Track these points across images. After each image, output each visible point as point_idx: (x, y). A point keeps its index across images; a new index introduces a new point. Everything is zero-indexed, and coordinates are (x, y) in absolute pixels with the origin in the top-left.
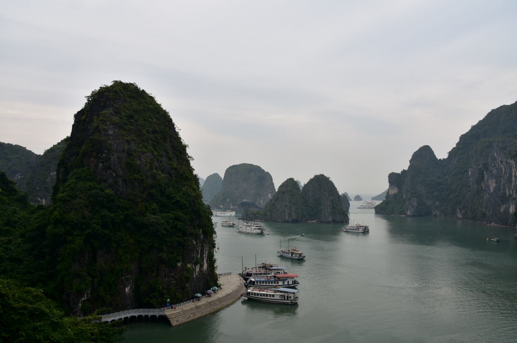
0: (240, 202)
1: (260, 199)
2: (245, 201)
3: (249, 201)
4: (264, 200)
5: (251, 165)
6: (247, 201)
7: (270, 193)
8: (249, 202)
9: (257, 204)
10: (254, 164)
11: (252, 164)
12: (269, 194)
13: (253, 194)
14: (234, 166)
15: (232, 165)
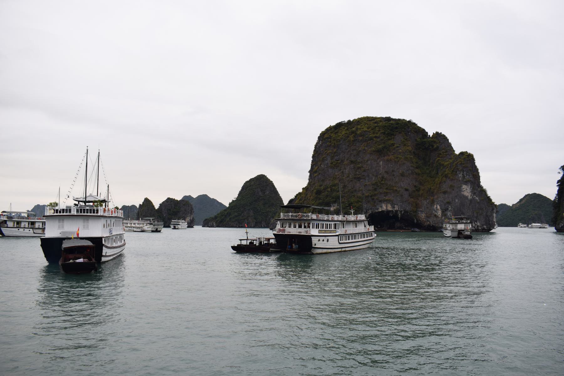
0: (370, 212)
1: (433, 203)
2: (384, 208)
3: (396, 208)
4: (449, 203)
5: (388, 119)
6: (390, 208)
7: (466, 183)
8: (397, 211)
9: (422, 216)
10: (393, 117)
11: (390, 117)
12: (464, 186)
13: (406, 190)
14: (340, 125)
15: (333, 124)
